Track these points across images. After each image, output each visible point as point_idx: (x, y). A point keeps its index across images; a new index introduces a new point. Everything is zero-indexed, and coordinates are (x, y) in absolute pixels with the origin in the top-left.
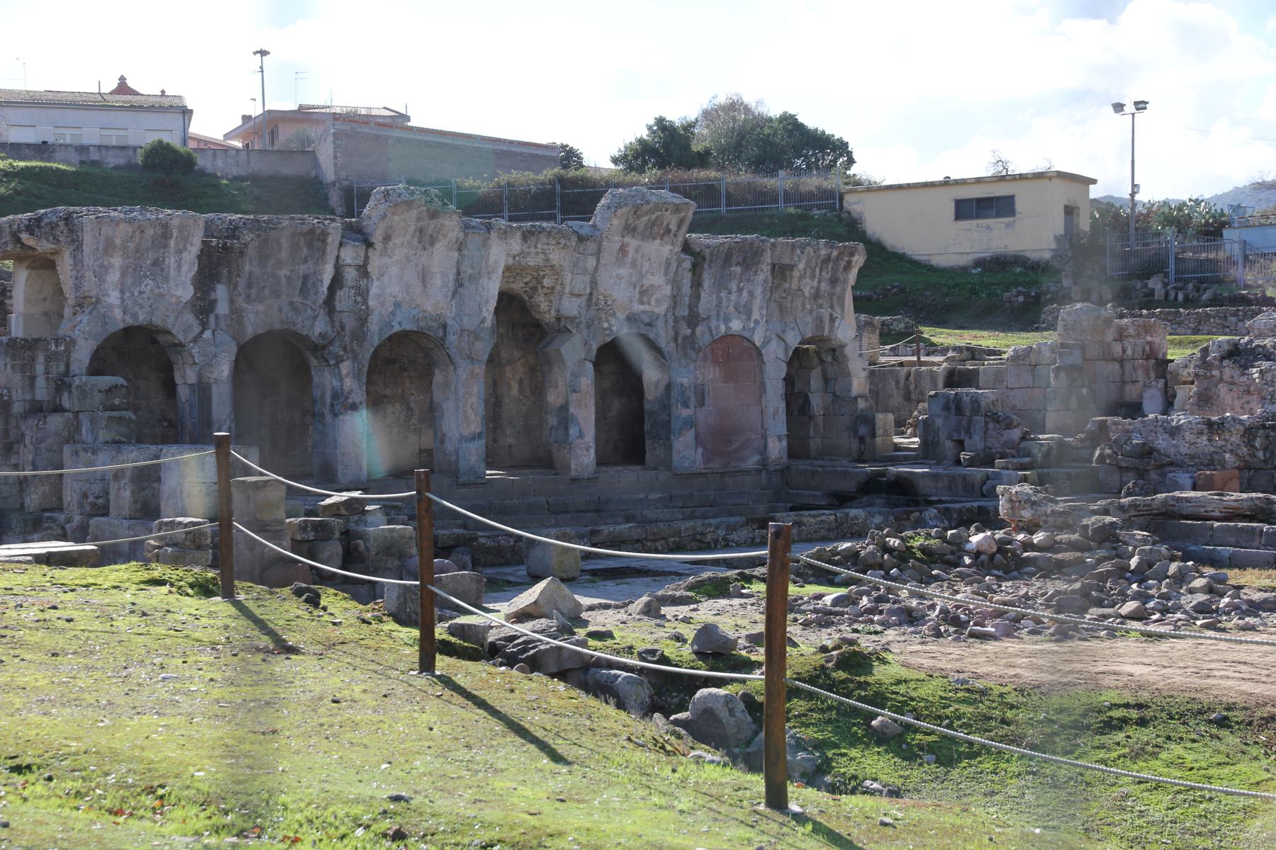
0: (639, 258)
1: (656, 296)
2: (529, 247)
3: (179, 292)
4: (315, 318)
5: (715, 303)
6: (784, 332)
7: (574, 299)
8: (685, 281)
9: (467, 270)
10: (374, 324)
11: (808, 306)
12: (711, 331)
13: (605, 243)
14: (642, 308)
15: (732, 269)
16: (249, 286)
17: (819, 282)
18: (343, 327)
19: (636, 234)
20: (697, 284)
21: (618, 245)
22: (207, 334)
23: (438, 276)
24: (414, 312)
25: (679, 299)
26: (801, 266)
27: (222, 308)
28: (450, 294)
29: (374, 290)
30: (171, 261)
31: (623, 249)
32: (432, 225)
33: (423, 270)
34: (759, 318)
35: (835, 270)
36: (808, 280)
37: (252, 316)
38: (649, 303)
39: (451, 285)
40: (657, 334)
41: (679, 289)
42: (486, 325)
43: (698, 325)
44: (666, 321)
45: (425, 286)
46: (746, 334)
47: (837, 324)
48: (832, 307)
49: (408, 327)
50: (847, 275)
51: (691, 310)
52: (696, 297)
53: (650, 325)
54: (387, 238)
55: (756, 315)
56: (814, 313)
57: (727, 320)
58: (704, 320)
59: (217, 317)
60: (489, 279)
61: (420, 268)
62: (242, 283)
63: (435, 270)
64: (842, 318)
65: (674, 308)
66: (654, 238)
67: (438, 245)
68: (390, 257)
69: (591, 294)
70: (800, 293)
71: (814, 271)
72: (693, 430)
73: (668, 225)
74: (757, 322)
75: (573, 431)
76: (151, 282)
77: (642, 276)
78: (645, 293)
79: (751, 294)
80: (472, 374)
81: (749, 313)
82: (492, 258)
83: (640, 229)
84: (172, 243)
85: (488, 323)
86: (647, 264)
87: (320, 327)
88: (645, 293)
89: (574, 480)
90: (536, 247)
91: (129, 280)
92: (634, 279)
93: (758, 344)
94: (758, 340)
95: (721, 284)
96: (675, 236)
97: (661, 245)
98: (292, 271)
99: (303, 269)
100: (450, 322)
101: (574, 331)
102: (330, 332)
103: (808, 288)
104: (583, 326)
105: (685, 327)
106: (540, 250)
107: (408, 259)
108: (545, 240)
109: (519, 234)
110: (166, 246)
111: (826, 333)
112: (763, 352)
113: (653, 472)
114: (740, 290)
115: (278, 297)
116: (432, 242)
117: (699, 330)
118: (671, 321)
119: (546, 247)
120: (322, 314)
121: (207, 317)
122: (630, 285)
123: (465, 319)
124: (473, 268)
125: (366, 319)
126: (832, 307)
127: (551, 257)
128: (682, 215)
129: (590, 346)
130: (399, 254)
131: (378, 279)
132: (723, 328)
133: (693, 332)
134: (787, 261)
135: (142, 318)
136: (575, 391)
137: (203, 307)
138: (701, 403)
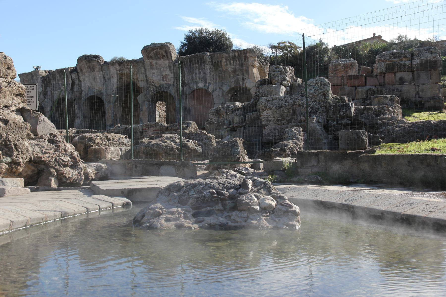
2: (122, 67)
6: (222, 86)
7: (142, 82)
9: (106, 76)
10: (83, 95)
11: (232, 75)
13: (145, 63)
14: (164, 82)
16: (53, 87)
20: (183, 72)
21: (149, 63)
22: (46, 100)
26: (224, 61)
27: (49, 93)
28: (103, 84)
29: (83, 85)
31: (151, 63)
32: (91, 65)
33: (94, 78)
34: (210, 82)
36: (229, 66)
37: (55, 94)
38: (166, 81)
40: (170, 91)
44: (174, 86)
46: (206, 88)
47: (246, 81)
48: (243, 75)
52: (183, 77)
54: (81, 70)
55: (209, 81)
56: (235, 78)
57: (197, 83)
60: (113, 78)
63: (98, 77)
64: (248, 78)
66: (160, 59)
67: (96, 70)
69: (146, 79)
71: (230, 62)
73: (162, 54)
74: (210, 84)
77: (161, 72)
79: (205, 73)
81: (205, 80)
83: (153, 56)
88: (164, 78)
92: (159, 73)
93: (210, 91)
94: (210, 90)
95: (191, 71)
96: (167, 57)
108: (126, 65)
109: (117, 64)
111: (241, 85)
112: (213, 94)
114: (200, 73)
116: (94, 70)
118: (176, 86)
119: (128, 67)
122: (158, 75)
126: (243, 75)
128: (164, 49)
130: (87, 74)
132: (195, 87)
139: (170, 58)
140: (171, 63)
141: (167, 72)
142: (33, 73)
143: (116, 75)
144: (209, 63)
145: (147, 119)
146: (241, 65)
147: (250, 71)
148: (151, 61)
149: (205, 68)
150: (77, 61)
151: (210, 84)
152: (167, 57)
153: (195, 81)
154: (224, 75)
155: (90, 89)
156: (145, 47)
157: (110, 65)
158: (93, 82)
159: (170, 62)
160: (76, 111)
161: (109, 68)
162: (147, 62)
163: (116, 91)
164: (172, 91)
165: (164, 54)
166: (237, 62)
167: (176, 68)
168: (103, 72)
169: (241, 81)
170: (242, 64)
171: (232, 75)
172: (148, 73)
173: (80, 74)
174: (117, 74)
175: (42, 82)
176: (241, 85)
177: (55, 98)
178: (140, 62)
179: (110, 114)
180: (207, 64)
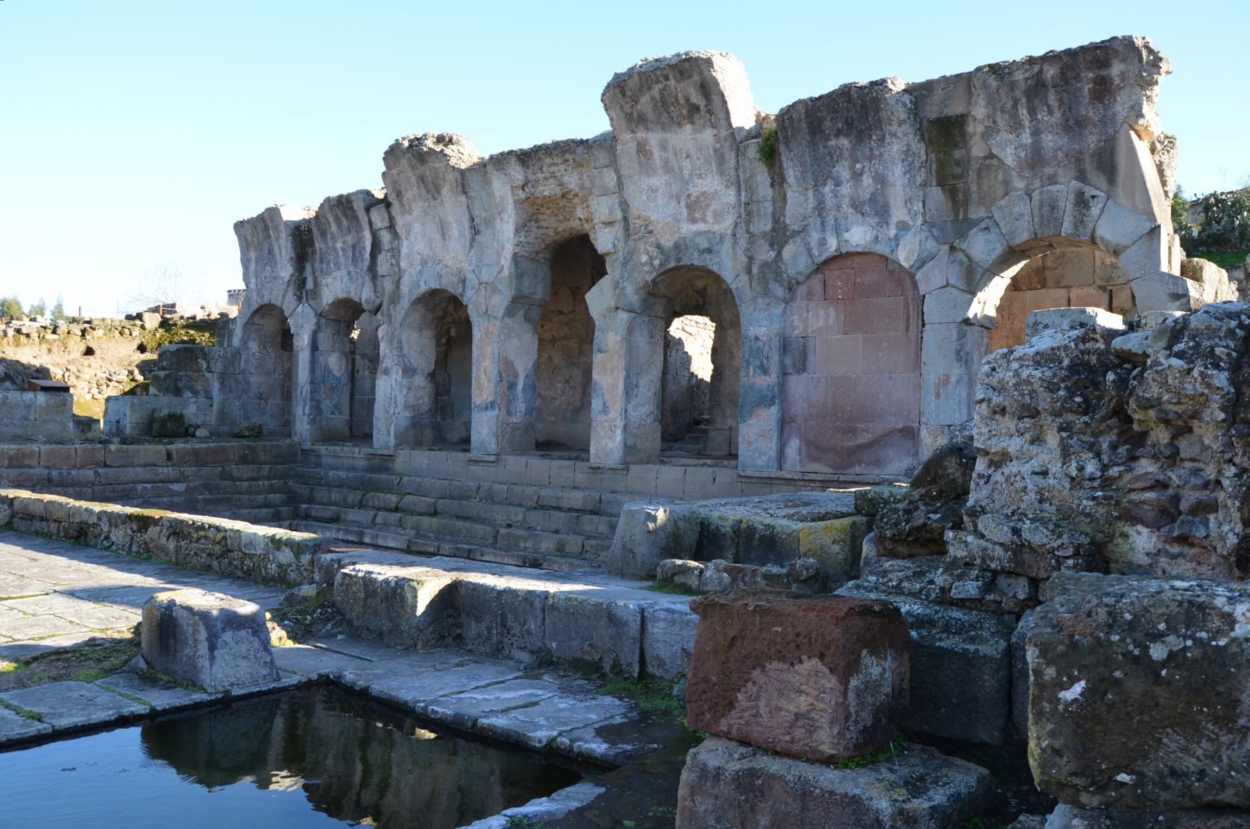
0: (671, 155)
1: (712, 208)
3: (283, 274)
4: (364, 284)
5: (812, 202)
8: (759, 178)
10: (405, 289)
11: (1020, 184)
12: (809, 250)
14: (694, 228)
15: (833, 143)
17: (1036, 133)
18: (384, 291)
19: (650, 125)
20: (778, 181)
21: (632, 147)
22: (300, 309)
23: (454, 225)
24: (439, 268)
25: (754, 207)
26: (980, 111)
27: (310, 285)
28: (468, 244)
29: (404, 251)
30: (276, 247)
34: (907, 219)
35: (1068, 106)
36: (1004, 136)
38: (704, 220)
39: (467, 233)
40: (719, 264)
41: (752, 191)
42: (503, 275)
43: (786, 242)
44: (735, 243)
45: (444, 239)
46: (882, 249)
47: (1095, 210)
48: (1082, 177)
49: (434, 285)
50: (1107, 107)
51: (776, 221)
52: (781, 199)
53: (709, 251)
54: (399, 194)
55: (898, 214)
56: (1036, 196)
57: (838, 231)
58: (795, 234)
59: (307, 292)
60: (502, 219)
61: (437, 220)
62: (317, 257)
63: (451, 219)
65: (748, 222)
66: (680, 125)
67: (445, 191)
68: (410, 213)
69: (625, 219)
70: (995, 162)
71: (1014, 116)
72: (774, 410)
73: (688, 100)
74: (903, 227)
75: (596, 404)
76: (269, 268)
77: (686, 183)
78: (694, 207)
79: (881, 180)
80: (487, 333)
82: (497, 194)
83: (650, 115)
84: (271, 232)
85: (506, 272)
86: (687, 164)
87: (365, 294)
88: (694, 207)
89: (595, 469)
90: (542, 172)
91: (259, 269)
92: (675, 188)
93: (905, 264)
94: (905, 256)
95: (820, 173)
96: (710, 112)
97: (696, 131)
98: (344, 242)
99: (350, 239)
100: (469, 276)
101: (609, 270)
102: (373, 297)
103: (1010, 150)
104: (618, 264)
105: (766, 247)
106: (548, 175)
107: (426, 214)
108: (548, 161)
109: (513, 159)
110: (269, 237)
112: (918, 276)
113: (710, 470)
114: (857, 176)
115: (339, 268)
116: (438, 192)
117: (788, 252)
118: (743, 243)
119: (554, 168)
120: (367, 278)
121: (301, 293)
122: (671, 196)
123: (484, 270)
124: (486, 211)
125: (399, 279)
127: (566, 179)
128: (696, 78)
129: (624, 289)
130: (417, 207)
131: (407, 239)
132: (832, 244)
133: (779, 254)
134: (957, 109)
135: (266, 301)
136: (600, 351)
137: (300, 283)
138: (802, 367)
139: (722, 116)
140: (725, 139)
141: (709, 180)
142: (266, 216)
143: (510, 207)
144: (904, 127)
145: (621, 386)
146: (1073, 126)
147: (1122, 160)
148: (641, 135)
149: (881, 155)
150: (384, 159)
151: (903, 227)
152: (710, 112)
153: (830, 221)
154: (979, 185)
155: (426, 263)
156: (617, 76)
157: (490, 167)
158: (437, 237)
159: (724, 133)
160: (383, 346)
161: (487, 182)
162: (627, 145)
163: (510, 268)
164: (728, 265)
165: (696, 99)
166: (1051, 118)
167: (747, 165)
168: (467, 198)
169: (1070, 207)
170: (1081, 123)
171: (1020, 184)
172: (631, 193)
173: (396, 210)
174: (516, 202)
175: (295, 248)
176: (1067, 227)
177: (325, 303)
178: (600, 145)
179: (488, 362)
180: (894, 135)
